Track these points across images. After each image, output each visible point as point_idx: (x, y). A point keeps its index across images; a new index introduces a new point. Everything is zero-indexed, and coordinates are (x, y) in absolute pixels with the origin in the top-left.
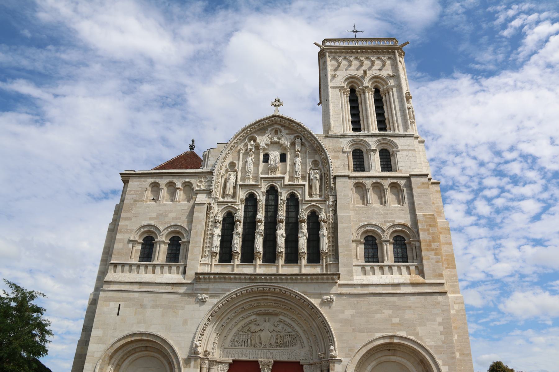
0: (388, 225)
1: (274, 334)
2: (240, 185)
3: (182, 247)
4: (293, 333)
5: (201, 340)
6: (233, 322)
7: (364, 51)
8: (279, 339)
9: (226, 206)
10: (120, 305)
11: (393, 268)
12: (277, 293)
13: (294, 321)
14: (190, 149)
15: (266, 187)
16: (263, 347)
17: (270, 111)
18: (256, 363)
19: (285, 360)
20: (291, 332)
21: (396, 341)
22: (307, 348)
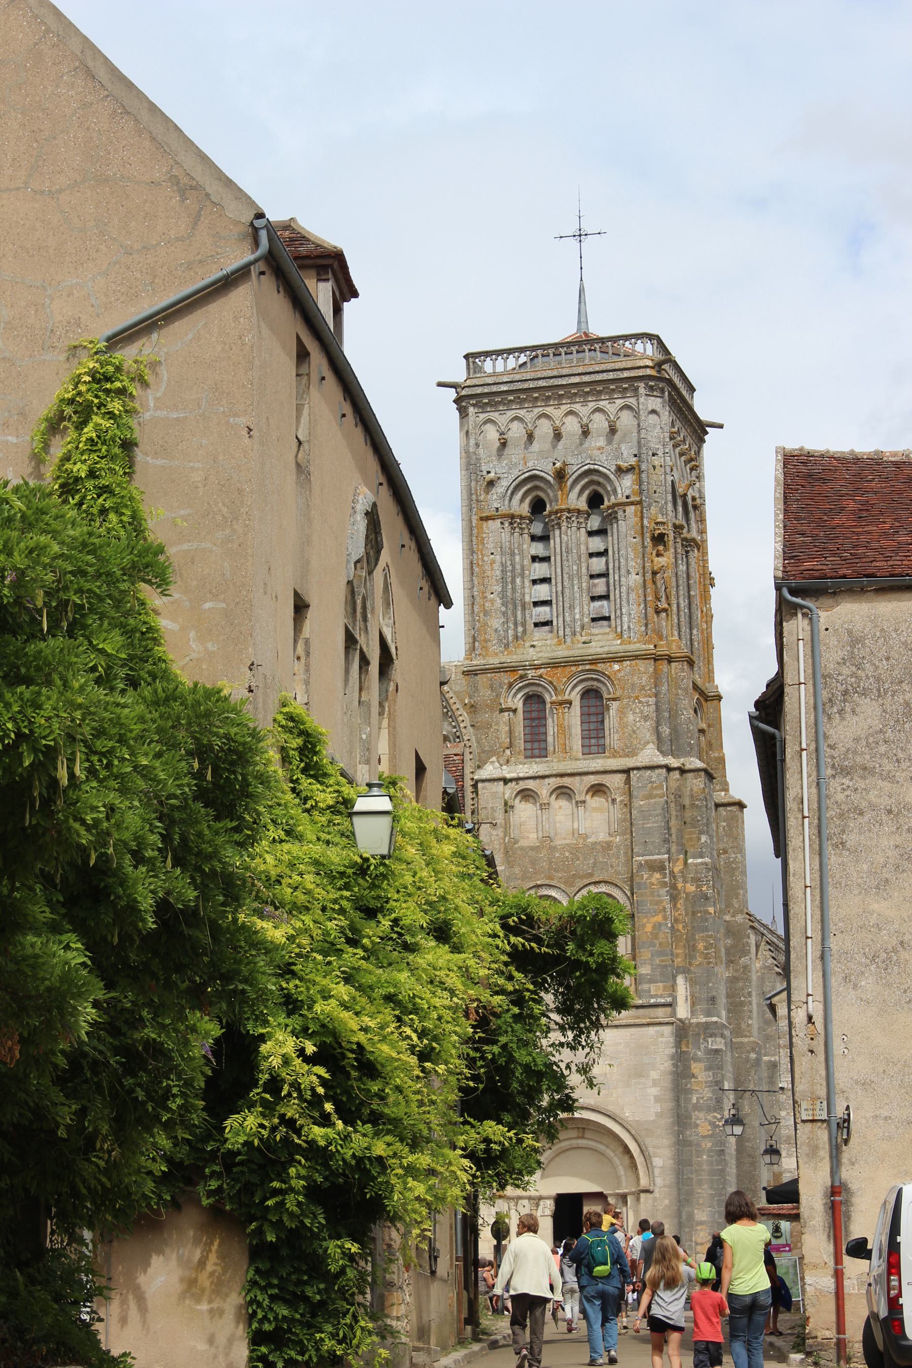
7: (562, 395)
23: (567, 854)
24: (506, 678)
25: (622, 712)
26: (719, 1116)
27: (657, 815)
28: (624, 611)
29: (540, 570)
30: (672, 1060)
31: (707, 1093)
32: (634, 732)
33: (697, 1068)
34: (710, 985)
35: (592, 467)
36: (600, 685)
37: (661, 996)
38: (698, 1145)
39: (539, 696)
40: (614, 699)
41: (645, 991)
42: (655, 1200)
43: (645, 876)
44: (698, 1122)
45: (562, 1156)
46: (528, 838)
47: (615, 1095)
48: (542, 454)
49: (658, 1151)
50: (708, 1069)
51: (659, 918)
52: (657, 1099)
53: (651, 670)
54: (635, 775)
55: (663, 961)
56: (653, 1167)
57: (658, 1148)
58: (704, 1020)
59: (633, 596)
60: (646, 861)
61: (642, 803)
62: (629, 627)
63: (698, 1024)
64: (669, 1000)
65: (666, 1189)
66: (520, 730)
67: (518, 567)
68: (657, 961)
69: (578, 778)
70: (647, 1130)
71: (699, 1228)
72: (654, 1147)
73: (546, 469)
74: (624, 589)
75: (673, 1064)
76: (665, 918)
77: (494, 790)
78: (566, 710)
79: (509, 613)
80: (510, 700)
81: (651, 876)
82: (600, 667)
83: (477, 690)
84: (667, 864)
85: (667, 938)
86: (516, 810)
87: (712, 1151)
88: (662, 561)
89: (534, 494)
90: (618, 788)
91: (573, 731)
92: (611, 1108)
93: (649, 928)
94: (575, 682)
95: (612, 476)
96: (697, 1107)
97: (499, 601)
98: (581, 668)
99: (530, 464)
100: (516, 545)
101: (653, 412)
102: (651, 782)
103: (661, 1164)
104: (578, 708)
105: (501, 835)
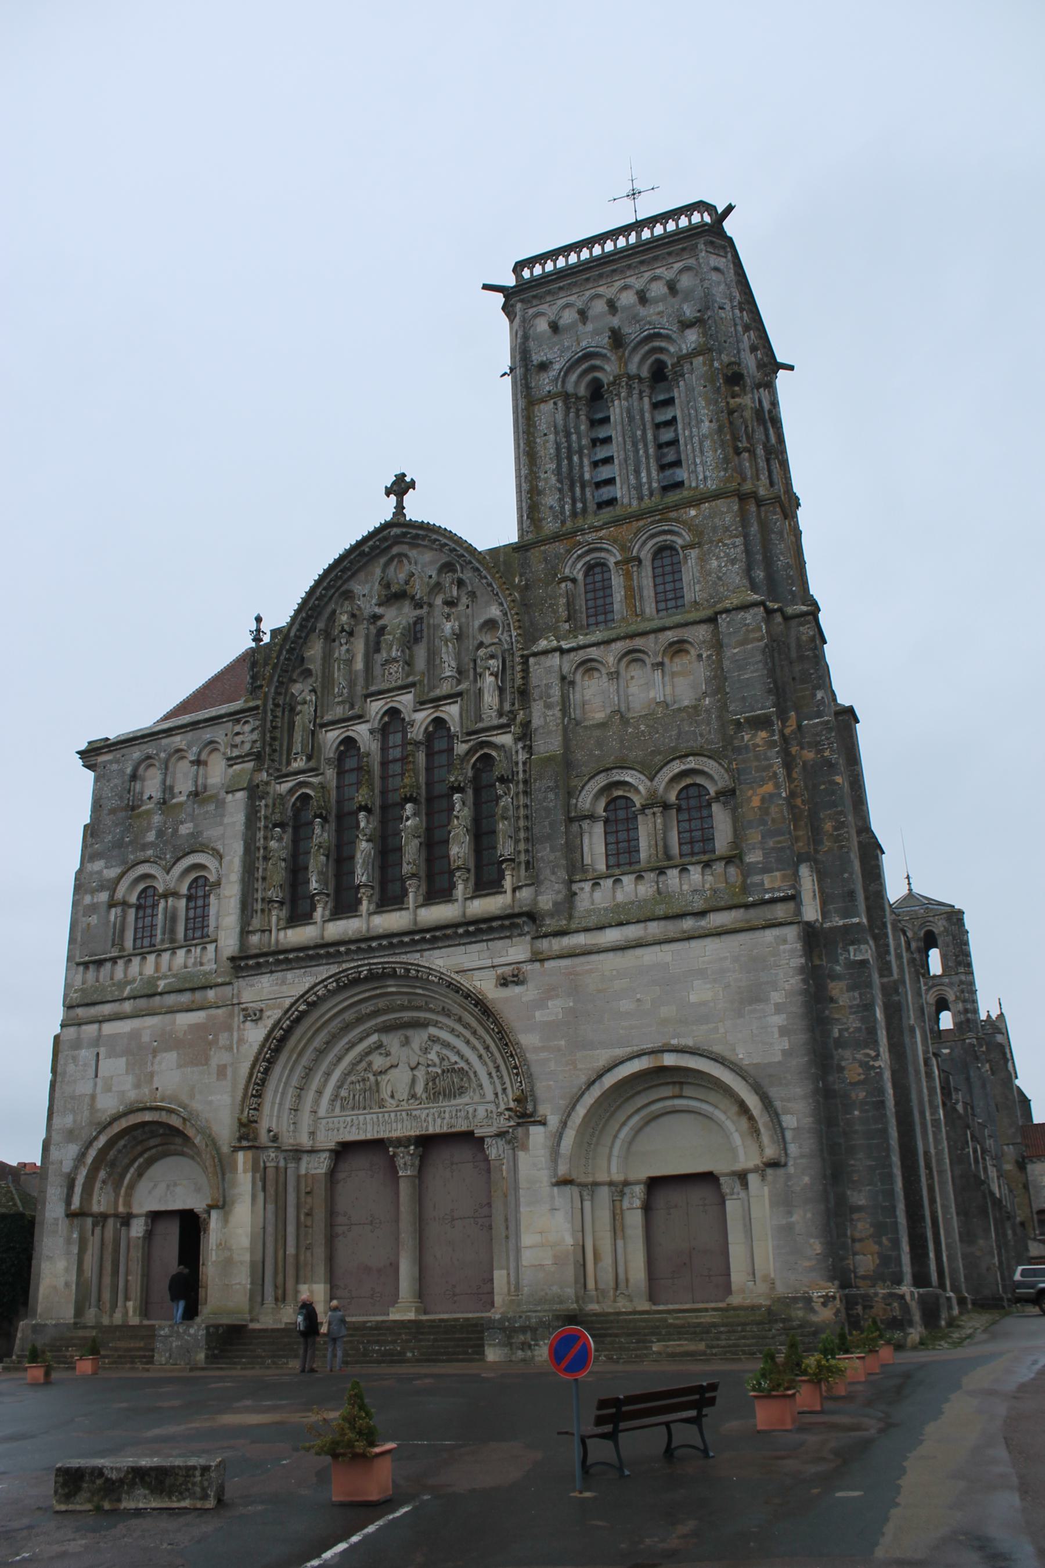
1: (420, 1074)
3: (212, 899)
4: (462, 1064)
5: (255, 1109)
6: (331, 1057)
8: (430, 1084)
9: (294, 783)
10: (98, 1054)
12: (401, 976)
13: (458, 1036)
14: (254, 640)
15: (379, 716)
16: (397, 1106)
17: (384, 510)
19: (445, 1130)
20: (456, 1063)
21: (669, 1060)
22: (490, 1096)
23: (643, 728)
24: (560, 548)
25: (702, 560)
27: (757, 663)
28: (698, 461)
29: (601, 453)
30: (801, 974)
31: (853, 1022)
32: (720, 578)
34: (846, 875)
35: (652, 331)
36: (674, 538)
37: (779, 890)
40: (691, 546)
42: (789, 1177)
43: (746, 738)
44: (843, 1064)
45: (653, 1124)
46: (594, 718)
47: (722, 1030)
48: (597, 332)
49: (789, 1105)
50: (851, 988)
51: (769, 788)
52: (783, 1031)
53: (736, 508)
54: (723, 620)
55: (779, 842)
58: (841, 923)
59: (707, 443)
60: (747, 719)
61: (736, 651)
62: (705, 478)
64: (790, 892)
65: (803, 1161)
66: (581, 603)
67: (575, 446)
68: (771, 843)
69: (652, 637)
71: (855, 1216)
74: (696, 440)
75: (805, 981)
76: (777, 786)
77: (548, 664)
78: (635, 569)
79: (566, 488)
80: (567, 570)
81: (754, 736)
82: (673, 515)
84: (774, 718)
85: (782, 811)
86: (578, 688)
89: (590, 377)
90: (704, 642)
91: (645, 593)
92: (717, 1049)
93: (756, 802)
94: (644, 538)
95: (674, 336)
96: (840, 1043)
97: (553, 479)
99: (584, 344)
100: (572, 425)
101: (716, 269)
102: (745, 625)
104: (650, 569)
105: (559, 714)
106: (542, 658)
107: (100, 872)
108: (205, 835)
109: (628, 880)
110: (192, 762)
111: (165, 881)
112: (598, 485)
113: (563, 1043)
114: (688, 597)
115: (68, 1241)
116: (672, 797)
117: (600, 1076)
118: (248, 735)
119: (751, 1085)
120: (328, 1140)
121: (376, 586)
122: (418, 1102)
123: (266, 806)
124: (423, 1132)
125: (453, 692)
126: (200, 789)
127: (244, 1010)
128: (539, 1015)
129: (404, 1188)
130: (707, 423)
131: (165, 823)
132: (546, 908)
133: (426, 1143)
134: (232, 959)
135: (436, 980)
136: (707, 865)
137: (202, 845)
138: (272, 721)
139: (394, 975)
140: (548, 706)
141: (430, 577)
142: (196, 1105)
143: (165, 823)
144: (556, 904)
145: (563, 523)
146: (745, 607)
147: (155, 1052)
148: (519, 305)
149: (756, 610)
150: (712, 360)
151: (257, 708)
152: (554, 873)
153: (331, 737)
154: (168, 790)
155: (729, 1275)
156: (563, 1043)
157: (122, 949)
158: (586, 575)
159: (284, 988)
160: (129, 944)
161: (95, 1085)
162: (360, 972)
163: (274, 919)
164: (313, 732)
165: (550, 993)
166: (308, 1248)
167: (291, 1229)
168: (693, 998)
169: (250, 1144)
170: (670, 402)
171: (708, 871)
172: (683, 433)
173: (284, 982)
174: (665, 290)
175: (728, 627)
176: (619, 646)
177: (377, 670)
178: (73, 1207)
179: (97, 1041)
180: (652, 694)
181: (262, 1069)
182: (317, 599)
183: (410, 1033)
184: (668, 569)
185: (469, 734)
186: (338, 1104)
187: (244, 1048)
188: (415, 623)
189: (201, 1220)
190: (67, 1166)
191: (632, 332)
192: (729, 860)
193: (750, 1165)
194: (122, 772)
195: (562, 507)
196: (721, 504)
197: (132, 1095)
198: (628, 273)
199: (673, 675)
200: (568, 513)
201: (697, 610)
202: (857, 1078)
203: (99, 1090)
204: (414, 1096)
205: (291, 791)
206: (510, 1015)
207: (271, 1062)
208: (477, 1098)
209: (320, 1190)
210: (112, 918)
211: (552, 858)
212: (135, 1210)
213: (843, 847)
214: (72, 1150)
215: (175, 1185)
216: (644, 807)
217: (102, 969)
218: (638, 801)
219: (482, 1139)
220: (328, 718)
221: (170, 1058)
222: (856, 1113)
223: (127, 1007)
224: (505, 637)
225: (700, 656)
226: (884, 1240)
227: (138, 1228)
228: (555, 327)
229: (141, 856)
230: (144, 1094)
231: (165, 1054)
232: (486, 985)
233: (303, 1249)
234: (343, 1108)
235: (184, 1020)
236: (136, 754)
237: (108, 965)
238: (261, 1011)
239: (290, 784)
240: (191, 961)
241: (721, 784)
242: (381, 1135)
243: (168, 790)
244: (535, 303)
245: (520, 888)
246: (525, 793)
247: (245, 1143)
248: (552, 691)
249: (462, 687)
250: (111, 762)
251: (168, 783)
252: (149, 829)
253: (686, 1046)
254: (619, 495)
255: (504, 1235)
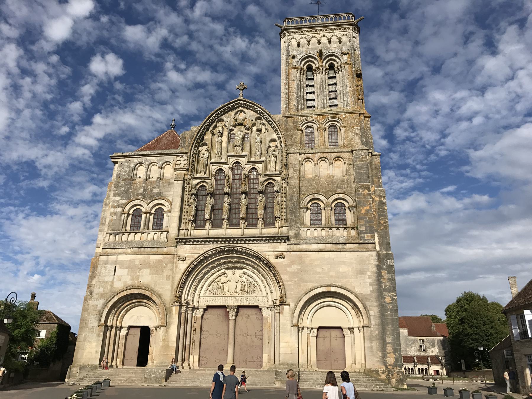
0: (331, 193)
2: (211, 163)
3: (165, 215)
6: (207, 276)
8: (243, 288)
10: (116, 267)
11: (333, 229)
15: (232, 163)
18: (224, 307)
19: (247, 304)
21: (333, 289)
22: (265, 294)
25: (346, 132)
26: (395, 295)
31: (389, 284)
32: (352, 139)
33: (384, 273)
34: (387, 238)
37: (370, 240)
38: (386, 307)
39: (312, 127)
40: (344, 127)
41: (363, 237)
42: (371, 331)
43: (361, 191)
44: (385, 296)
46: (308, 177)
47: (350, 282)
48: (313, 49)
49: (372, 308)
50: (388, 273)
51: (368, 208)
52: (371, 284)
56: (370, 316)
57: (372, 307)
58: (385, 252)
59: (349, 94)
61: (358, 163)
63: (384, 254)
65: (377, 326)
69: (330, 154)
70: (366, 298)
71: (388, 345)
72: (370, 306)
73: (315, 53)
76: (371, 207)
77: (295, 157)
79: (300, 99)
80: (300, 127)
81: (363, 191)
82: (339, 116)
83: (287, 123)
87: (392, 310)
88: (359, 83)
92: (349, 287)
93: (363, 211)
95: (339, 56)
97: (295, 96)
98: (329, 116)
99: (308, 52)
101: (354, 37)
103: (374, 315)
105: (298, 173)
106: (292, 154)
107: (118, 201)
108: (164, 193)
109: (319, 229)
110: (159, 167)
111: (146, 208)
112: (308, 100)
113: (296, 279)
114: (340, 143)
115: (98, 335)
116: (333, 205)
117: (309, 292)
118: (183, 161)
119: (360, 301)
120: (203, 304)
121: (232, 119)
122: (238, 294)
123: (189, 187)
124: (239, 305)
125: (260, 160)
126: (162, 177)
127: (179, 256)
128: (288, 269)
129: (232, 323)
130: (349, 88)
131: (147, 187)
132: (292, 235)
133: (239, 307)
134: (176, 239)
135: (253, 254)
136: (345, 229)
137: (162, 196)
138: (192, 159)
139: (237, 251)
140: (295, 171)
141: (252, 120)
142: (157, 289)
143: (147, 187)
144: (295, 234)
145: (298, 111)
146: (362, 150)
147: (140, 268)
148: (287, 33)
149: (365, 151)
150: (352, 68)
151: (187, 153)
152: (295, 224)
153: (215, 168)
154: (148, 176)
155: (345, 361)
156: (296, 279)
157: (126, 230)
158: (305, 129)
159: (195, 250)
160: (128, 227)
161: (114, 278)
162: (225, 248)
163: (190, 226)
164: (207, 165)
165: (293, 262)
166: (194, 342)
167: (188, 335)
168: (341, 270)
169: (179, 304)
170: (335, 77)
171: (345, 230)
172: (339, 89)
173: (195, 248)
174: (338, 40)
175: (356, 155)
176: (319, 155)
177: (231, 148)
178: (101, 323)
179: (116, 262)
180: (329, 172)
181: (185, 278)
182: (211, 120)
183: (236, 270)
184: (334, 132)
185: (265, 175)
186: (208, 291)
187: (178, 270)
188: (245, 135)
189: (151, 330)
190: (100, 307)
191: (325, 53)
192: (353, 229)
193: (356, 325)
194: (129, 166)
195: (298, 106)
196: (354, 116)
197: (130, 283)
198: (325, 32)
199: (335, 167)
200: (300, 108)
201: (344, 148)
202: (389, 302)
203: (115, 279)
204: (236, 292)
205: (198, 183)
206: (279, 269)
207: (188, 276)
208: (259, 295)
209: (199, 322)
210: (123, 218)
211: (295, 219)
212: (123, 325)
213: (386, 229)
214: (102, 301)
215: (141, 317)
216: (324, 208)
217: (117, 236)
218: (322, 205)
219: (261, 309)
220: (213, 160)
221: (148, 271)
222: (389, 312)
223: (129, 250)
224: (279, 145)
225: (345, 163)
226: (397, 353)
227: (124, 332)
228: (299, 45)
229: (136, 197)
230: (136, 282)
231: (144, 269)
232: (271, 258)
233: (191, 343)
234: (209, 294)
235: (153, 258)
236: (136, 160)
237: (121, 235)
238: (186, 258)
239: (198, 181)
240: (156, 237)
241: (351, 203)
242: (224, 304)
243: (148, 176)
244: (292, 34)
245: (282, 227)
246: (285, 197)
247: (176, 304)
248: (296, 166)
249: (263, 159)
250: (125, 162)
251: (148, 173)
252: (140, 188)
253: (338, 285)
254: (316, 105)
255: (267, 342)
